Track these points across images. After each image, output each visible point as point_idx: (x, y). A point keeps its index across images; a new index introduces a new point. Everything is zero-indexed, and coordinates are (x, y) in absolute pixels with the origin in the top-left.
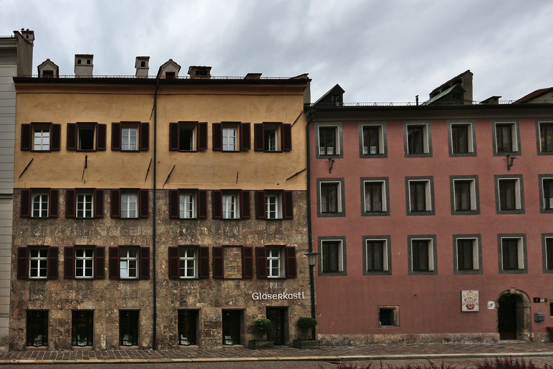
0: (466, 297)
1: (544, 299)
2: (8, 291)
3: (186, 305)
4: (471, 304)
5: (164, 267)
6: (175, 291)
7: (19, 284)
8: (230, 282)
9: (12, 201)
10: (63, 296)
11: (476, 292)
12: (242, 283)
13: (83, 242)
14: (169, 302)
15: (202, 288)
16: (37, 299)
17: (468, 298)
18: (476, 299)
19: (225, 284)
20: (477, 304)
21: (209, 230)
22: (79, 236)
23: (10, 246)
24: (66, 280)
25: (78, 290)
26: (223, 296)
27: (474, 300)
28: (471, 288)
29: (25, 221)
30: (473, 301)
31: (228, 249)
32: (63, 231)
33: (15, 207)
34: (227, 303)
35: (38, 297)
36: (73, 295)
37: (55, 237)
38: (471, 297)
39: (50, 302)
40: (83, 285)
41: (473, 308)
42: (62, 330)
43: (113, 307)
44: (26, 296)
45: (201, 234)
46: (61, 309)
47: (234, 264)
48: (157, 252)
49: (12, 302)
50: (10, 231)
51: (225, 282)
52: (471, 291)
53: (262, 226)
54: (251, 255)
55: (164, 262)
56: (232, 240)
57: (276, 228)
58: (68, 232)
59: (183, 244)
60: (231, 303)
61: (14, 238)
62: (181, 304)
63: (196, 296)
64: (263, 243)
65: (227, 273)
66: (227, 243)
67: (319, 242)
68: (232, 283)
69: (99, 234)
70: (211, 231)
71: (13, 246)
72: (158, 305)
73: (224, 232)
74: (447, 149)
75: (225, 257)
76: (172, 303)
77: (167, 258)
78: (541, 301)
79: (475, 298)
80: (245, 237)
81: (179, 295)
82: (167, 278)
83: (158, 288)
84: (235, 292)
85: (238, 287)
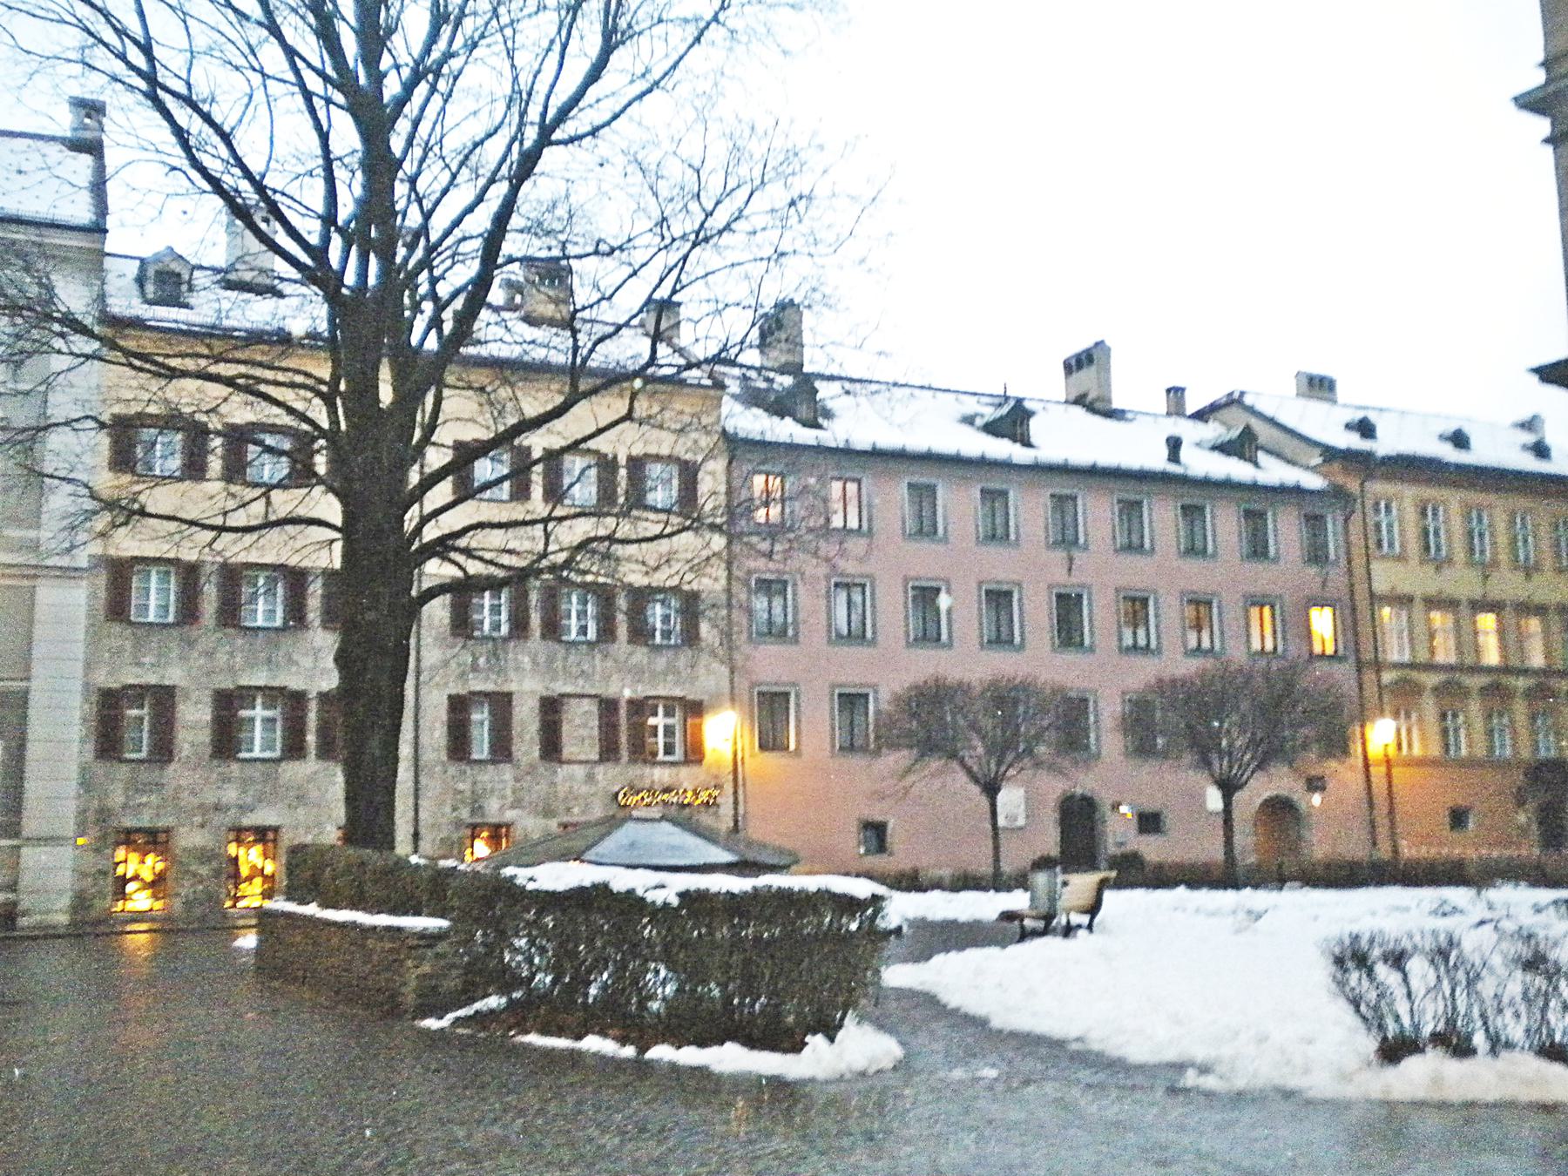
2: (72, 787)
3: (483, 815)
5: (437, 734)
6: (461, 786)
7: (100, 768)
8: (576, 767)
9: (84, 583)
10: (210, 797)
12: (600, 771)
13: (260, 678)
14: (448, 809)
15: (517, 780)
16: (145, 805)
19: (563, 771)
21: (534, 662)
22: (251, 664)
23: (77, 686)
24: (215, 762)
25: (245, 783)
26: (561, 795)
29: (116, 628)
31: (573, 701)
32: (210, 654)
33: (93, 596)
34: (568, 810)
35: (144, 799)
36: (231, 794)
37: (191, 667)
39: (179, 810)
40: (256, 771)
42: (204, 871)
43: (323, 819)
44: (117, 798)
45: (517, 669)
46: (202, 826)
47: (584, 732)
48: (424, 704)
49: (82, 812)
50: (79, 650)
51: (565, 766)
53: (640, 655)
54: (616, 710)
55: (437, 725)
56: (581, 682)
57: (668, 663)
58: (222, 658)
59: (478, 688)
60: (576, 810)
61: (89, 666)
62: (473, 812)
63: (503, 797)
64: (642, 691)
65: (568, 751)
66: (569, 689)
67: (751, 693)
68: (579, 771)
69: (291, 661)
70: (538, 664)
71: (86, 685)
72: (423, 815)
73: (564, 667)
75: (564, 716)
76: (455, 809)
77: (445, 717)
80: (607, 678)
81: (468, 794)
82: (445, 758)
83: (423, 780)
84: (584, 789)
85: (590, 778)
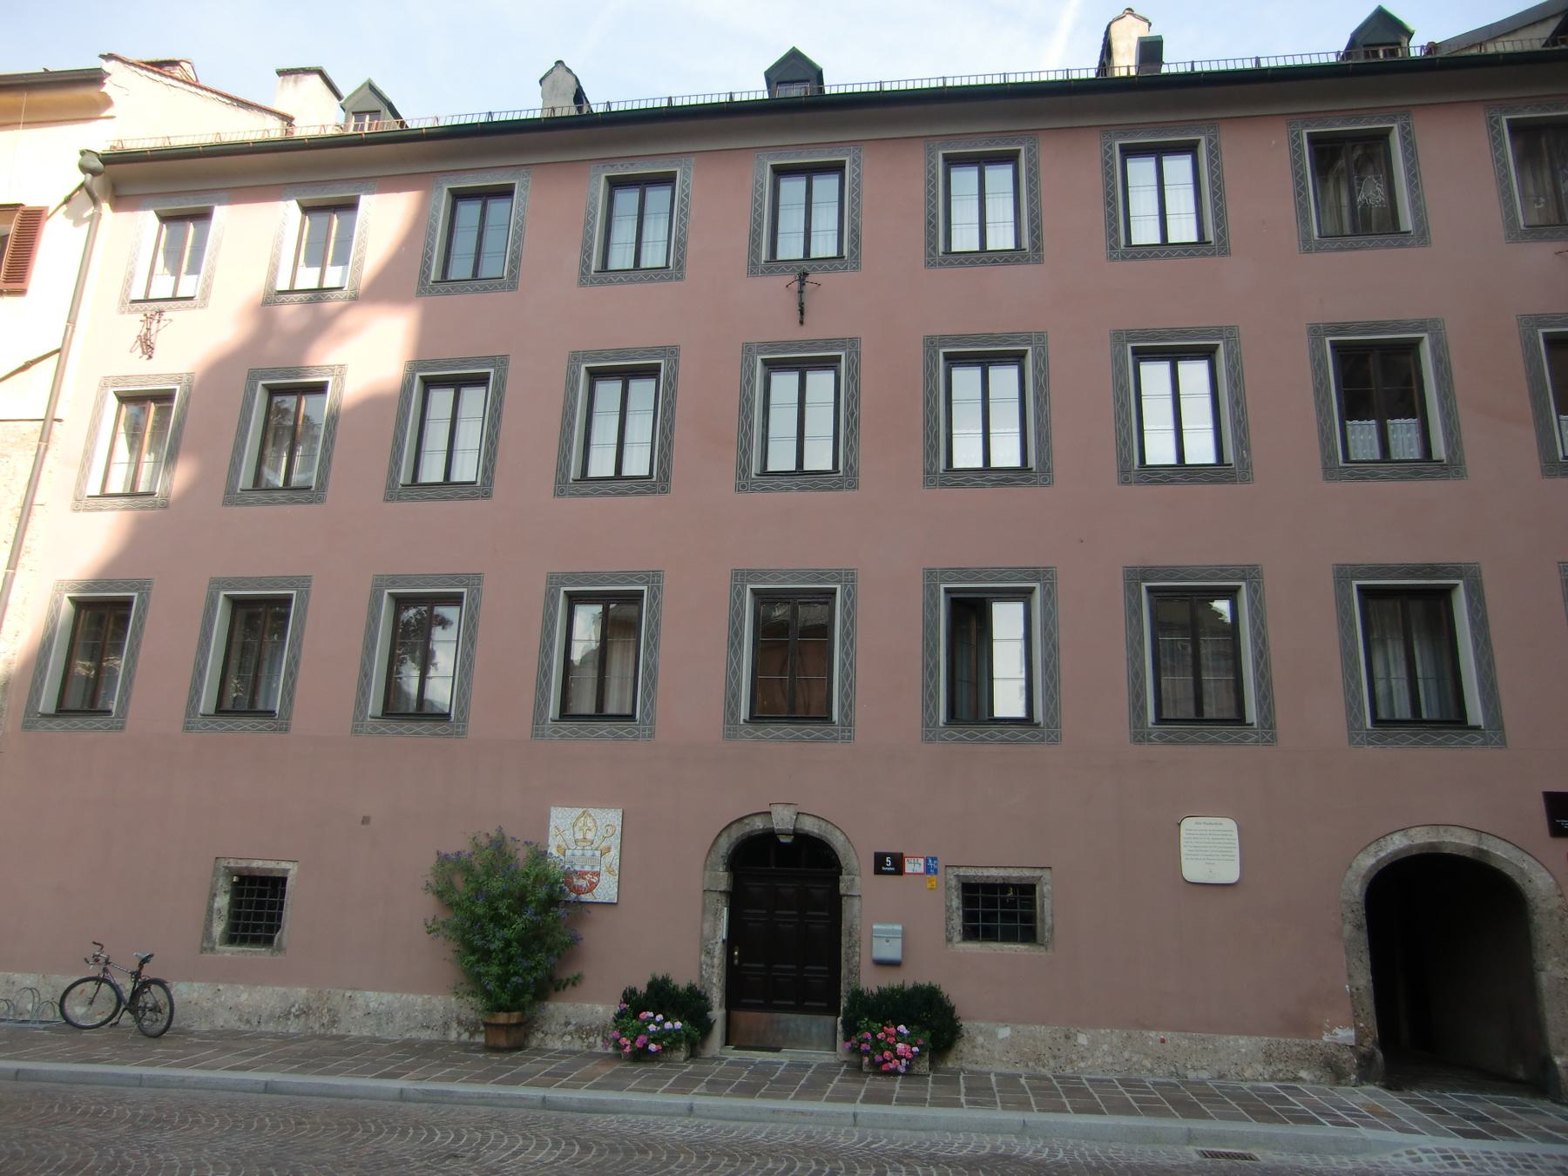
0: (568, 835)
1: (921, 861)
4: (587, 868)
11: (613, 817)
17: (576, 841)
18: (609, 849)
20: (610, 872)
27: (598, 853)
28: (582, 796)
30: (593, 855)
38: (590, 836)
41: (592, 886)
52: (591, 811)
74: (575, 258)
78: (909, 868)
79: (604, 844)
